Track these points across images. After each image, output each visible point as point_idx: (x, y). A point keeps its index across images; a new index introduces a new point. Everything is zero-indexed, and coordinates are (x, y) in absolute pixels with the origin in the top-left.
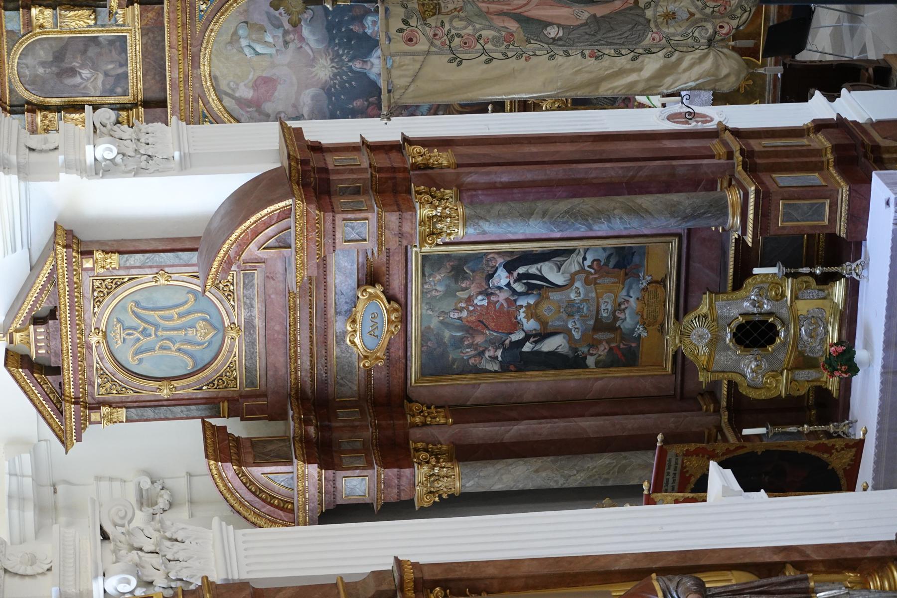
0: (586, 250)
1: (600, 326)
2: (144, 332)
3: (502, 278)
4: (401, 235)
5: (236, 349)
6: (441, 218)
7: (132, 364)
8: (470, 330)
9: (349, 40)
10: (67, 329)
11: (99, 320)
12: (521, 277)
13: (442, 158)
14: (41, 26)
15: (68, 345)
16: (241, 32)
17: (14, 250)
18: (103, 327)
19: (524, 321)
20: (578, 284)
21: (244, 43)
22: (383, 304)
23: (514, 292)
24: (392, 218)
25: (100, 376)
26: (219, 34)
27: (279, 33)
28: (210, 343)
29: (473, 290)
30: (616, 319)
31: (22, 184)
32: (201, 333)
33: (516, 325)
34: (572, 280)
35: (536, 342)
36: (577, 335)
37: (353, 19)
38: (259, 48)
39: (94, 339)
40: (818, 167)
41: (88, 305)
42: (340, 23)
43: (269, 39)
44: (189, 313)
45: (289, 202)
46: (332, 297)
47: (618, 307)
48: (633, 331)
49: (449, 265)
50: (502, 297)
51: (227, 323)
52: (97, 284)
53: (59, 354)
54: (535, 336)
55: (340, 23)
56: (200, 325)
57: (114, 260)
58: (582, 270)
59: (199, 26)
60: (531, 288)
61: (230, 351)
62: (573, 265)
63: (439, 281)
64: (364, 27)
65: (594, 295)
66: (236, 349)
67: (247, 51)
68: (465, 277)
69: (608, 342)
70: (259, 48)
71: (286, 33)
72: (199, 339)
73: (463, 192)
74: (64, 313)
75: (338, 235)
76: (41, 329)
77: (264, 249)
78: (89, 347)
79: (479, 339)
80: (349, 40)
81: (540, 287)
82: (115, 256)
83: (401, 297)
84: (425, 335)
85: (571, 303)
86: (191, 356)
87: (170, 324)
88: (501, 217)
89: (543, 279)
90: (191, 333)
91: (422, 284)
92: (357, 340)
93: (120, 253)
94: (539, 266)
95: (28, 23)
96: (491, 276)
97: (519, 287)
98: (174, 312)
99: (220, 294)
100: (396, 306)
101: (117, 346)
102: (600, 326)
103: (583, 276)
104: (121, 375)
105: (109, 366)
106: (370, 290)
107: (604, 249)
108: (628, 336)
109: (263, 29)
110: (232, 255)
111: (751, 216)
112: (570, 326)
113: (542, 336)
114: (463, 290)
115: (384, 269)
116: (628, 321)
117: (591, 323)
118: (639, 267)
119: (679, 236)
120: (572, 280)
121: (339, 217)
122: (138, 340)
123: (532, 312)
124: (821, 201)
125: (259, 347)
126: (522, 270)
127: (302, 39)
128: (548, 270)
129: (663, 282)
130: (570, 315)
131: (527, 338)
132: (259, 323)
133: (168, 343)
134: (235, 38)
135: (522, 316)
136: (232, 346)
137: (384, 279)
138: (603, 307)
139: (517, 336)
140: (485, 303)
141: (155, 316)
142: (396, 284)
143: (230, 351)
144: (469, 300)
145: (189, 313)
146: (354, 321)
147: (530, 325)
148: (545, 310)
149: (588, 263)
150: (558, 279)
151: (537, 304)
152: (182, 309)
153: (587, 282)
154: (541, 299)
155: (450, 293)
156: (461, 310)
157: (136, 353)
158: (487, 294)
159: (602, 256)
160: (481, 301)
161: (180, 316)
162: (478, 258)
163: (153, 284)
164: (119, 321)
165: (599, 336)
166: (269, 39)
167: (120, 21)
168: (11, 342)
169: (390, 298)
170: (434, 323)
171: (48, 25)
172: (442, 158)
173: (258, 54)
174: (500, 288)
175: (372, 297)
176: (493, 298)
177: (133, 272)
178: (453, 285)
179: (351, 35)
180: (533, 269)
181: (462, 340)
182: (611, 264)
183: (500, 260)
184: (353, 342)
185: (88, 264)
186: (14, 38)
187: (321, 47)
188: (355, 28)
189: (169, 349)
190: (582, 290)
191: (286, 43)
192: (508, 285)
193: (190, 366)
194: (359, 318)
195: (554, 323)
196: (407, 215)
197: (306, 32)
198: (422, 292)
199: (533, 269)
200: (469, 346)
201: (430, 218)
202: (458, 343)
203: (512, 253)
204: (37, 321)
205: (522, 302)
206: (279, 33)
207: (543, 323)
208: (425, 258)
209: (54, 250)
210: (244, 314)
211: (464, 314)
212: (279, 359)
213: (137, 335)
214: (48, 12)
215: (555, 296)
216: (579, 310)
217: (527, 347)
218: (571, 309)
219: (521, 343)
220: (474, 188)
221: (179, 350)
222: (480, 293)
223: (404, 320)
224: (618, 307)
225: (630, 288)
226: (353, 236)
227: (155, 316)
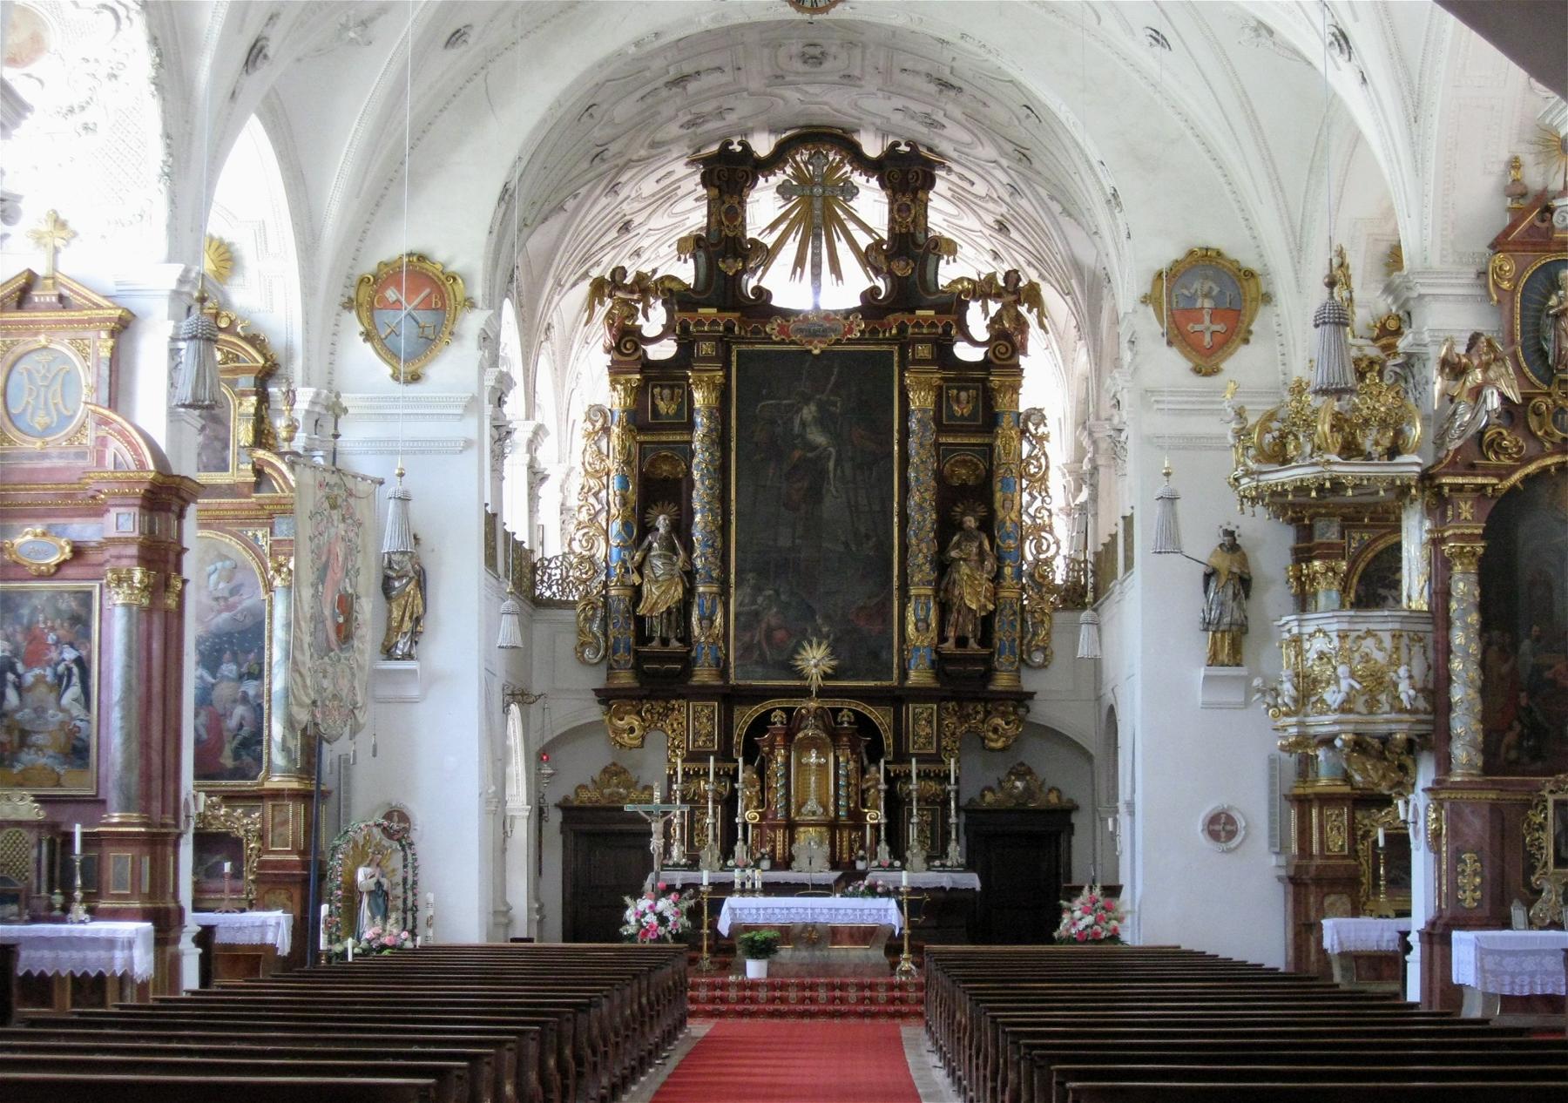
0: (88, 722)
1: (24, 735)
2: (45, 377)
3: (69, 654)
4: (119, 557)
5: (25, 445)
6: (131, 587)
7: (20, 367)
8: (29, 630)
9: (217, 651)
10: (54, 316)
11: (58, 343)
12: (69, 670)
13: (171, 602)
14: (240, 404)
15: (40, 316)
16: (228, 563)
17: (117, 284)
18: (52, 346)
19: (33, 673)
20: (61, 716)
21: (219, 565)
22: (54, 559)
23: (57, 664)
24: (133, 550)
25: (12, 342)
26: (227, 544)
27: (226, 594)
28: (31, 427)
29: (61, 632)
30: (29, 747)
31: (168, 293)
32: (40, 420)
33: (29, 665)
34: (62, 710)
35: (14, 683)
36: (18, 716)
37: (234, 654)
38: (214, 578)
39: (42, 339)
40: (152, 895)
41: (72, 335)
42: (231, 643)
43: (222, 585)
44: (57, 410)
45: (152, 467)
46: (62, 521)
47: (39, 749)
48: (18, 761)
49: (83, 612)
50: (54, 655)
51: (48, 439)
52: (86, 342)
53: (35, 309)
54: (20, 682)
55: (231, 643)
56: (47, 420)
57: (105, 353)
58: (73, 718)
59: (234, 529)
60: (59, 678)
61: (24, 441)
62: (77, 711)
63: (69, 604)
64: (229, 662)
65: (51, 728)
66: (25, 445)
67: (212, 568)
68: (72, 625)
69: (11, 742)
70: (214, 578)
71: (226, 599)
72: (37, 419)
73: (149, 611)
74: (66, 315)
75: (122, 510)
76: (54, 299)
77: (115, 456)
78: (37, 334)
79: (19, 638)
80: (217, 651)
81: (60, 684)
82: (108, 355)
83: (59, 575)
84: (27, 594)
85: (44, 710)
86: (25, 410)
87: (50, 396)
88: (129, 632)
89: (68, 686)
90: (42, 413)
91: (68, 592)
92: (29, 537)
93: (111, 360)
94: (79, 685)
95: (243, 394)
96: (72, 645)
97: (61, 668)
98: (59, 400)
99: (72, 434)
100: (52, 570)
101: (35, 357)
102: (24, 735)
103: (67, 719)
104: (11, 358)
105: (19, 349)
106: (68, 549)
107: (88, 736)
108: (14, 758)
109: (229, 580)
110: (114, 425)
111: (120, 829)
112: (27, 710)
113: (19, 687)
114: (62, 626)
115: (82, 562)
116: (27, 757)
117: (28, 728)
118: (71, 764)
119: (97, 795)
120: (62, 710)
121: (136, 510)
122: (38, 372)
123: (40, 680)
124: (129, 886)
125: (27, 465)
126: (75, 670)
127: (220, 612)
128: (74, 691)
129: (58, 784)
130: (35, 710)
131: (19, 676)
132: (46, 464)
133: (35, 394)
134: (225, 558)
135: (37, 671)
136: (29, 442)
137: (75, 562)
138: (40, 736)
139: (20, 667)
140: (50, 642)
141: (57, 386)
142: (69, 571)
143: (24, 441)
144: (53, 629)
145: (57, 410)
146: (44, 534)
147: (29, 678)
148: (42, 689)
149: (78, 723)
150: (67, 698)
151: (46, 682)
152: (61, 406)
153: (62, 723)
154: (51, 687)
155: (59, 612)
156: (45, 623)
157: (29, 373)
158: (58, 643)
159: (82, 735)
160: (51, 638)
161: (55, 404)
162: (87, 636)
163: (84, 384)
164: (55, 358)
165: (16, 734)
166: (222, 585)
167: (241, 466)
168: (46, 278)
169: (59, 566)
170: (36, 602)
171: (242, 409)
172: (171, 602)
173: (210, 575)
174: (61, 653)
175: (62, 548)
176: (53, 648)
177: (95, 369)
178: (66, 616)
179: (220, 651)
180: (75, 679)
181: (21, 624)
182: (76, 742)
183: (84, 653)
184: (27, 533)
185: (104, 335)
186: (232, 384)
187: (213, 627)
188: (227, 655)
189: (30, 395)
190: (55, 719)
191: (217, 599)
192: (64, 660)
193: (13, 411)
194: (45, 539)
195: (29, 698)
196: (135, 561)
197: (225, 615)
198: (62, 592)
199: (75, 679)
200: (15, 631)
201: (131, 579)
202: (18, 619)
203: (89, 661)
204: (61, 298)
205: (49, 672)
206: (226, 594)
207: (30, 689)
208: (89, 594)
209: (119, 308)
210: (54, 452)
211: (42, 626)
212: (16, 479)
213: (43, 372)
214: (252, 410)
215: (52, 697)
216: (39, 717)
217: (10, 677)
218: (40, 711)
219: (13, 669)
220: (150, 623)
221: (28, 403)
222: (58, 638)
223: (41, 577)
224: (39, 749)
225: (55, 758)
226: (121, 520)
227: (57, 386)
